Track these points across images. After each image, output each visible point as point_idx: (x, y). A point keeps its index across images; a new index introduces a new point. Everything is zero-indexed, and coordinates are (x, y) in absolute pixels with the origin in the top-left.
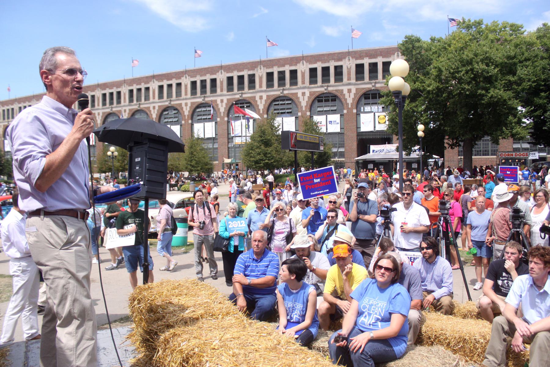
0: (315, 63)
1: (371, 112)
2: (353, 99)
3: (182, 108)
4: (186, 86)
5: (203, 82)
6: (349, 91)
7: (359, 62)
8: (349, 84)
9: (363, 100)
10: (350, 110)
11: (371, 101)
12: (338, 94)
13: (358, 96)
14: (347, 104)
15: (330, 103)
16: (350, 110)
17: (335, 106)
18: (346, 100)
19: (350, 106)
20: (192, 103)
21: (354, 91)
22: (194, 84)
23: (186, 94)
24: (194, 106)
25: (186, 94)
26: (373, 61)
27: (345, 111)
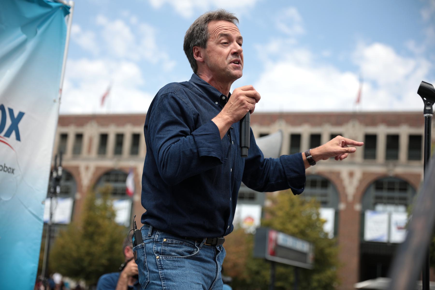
0: (300, 124)
1: (383, 212)
2: (357, 189)
3: (79, 174)
4: (91, 140)
5: (120, 138)
6: (351, 174)
7: (371, 130)
8: (352, 163)
9: (373, 193)
10: (350, 205)
11: (385, 194)
12: (333, 178)
13: (365, 184)
14: (346, 196)
15: (318, 191)
16: (350, 205)
17: (325, 195)
18: (344, 188)
19: (350, 198)
20: (98, 168)
21: (358, 175)
22: (104, 138)
23: (89, 151)
24: (100, 172)
25: (89, 151)
26: (393, 131)
27: (342, 206)
